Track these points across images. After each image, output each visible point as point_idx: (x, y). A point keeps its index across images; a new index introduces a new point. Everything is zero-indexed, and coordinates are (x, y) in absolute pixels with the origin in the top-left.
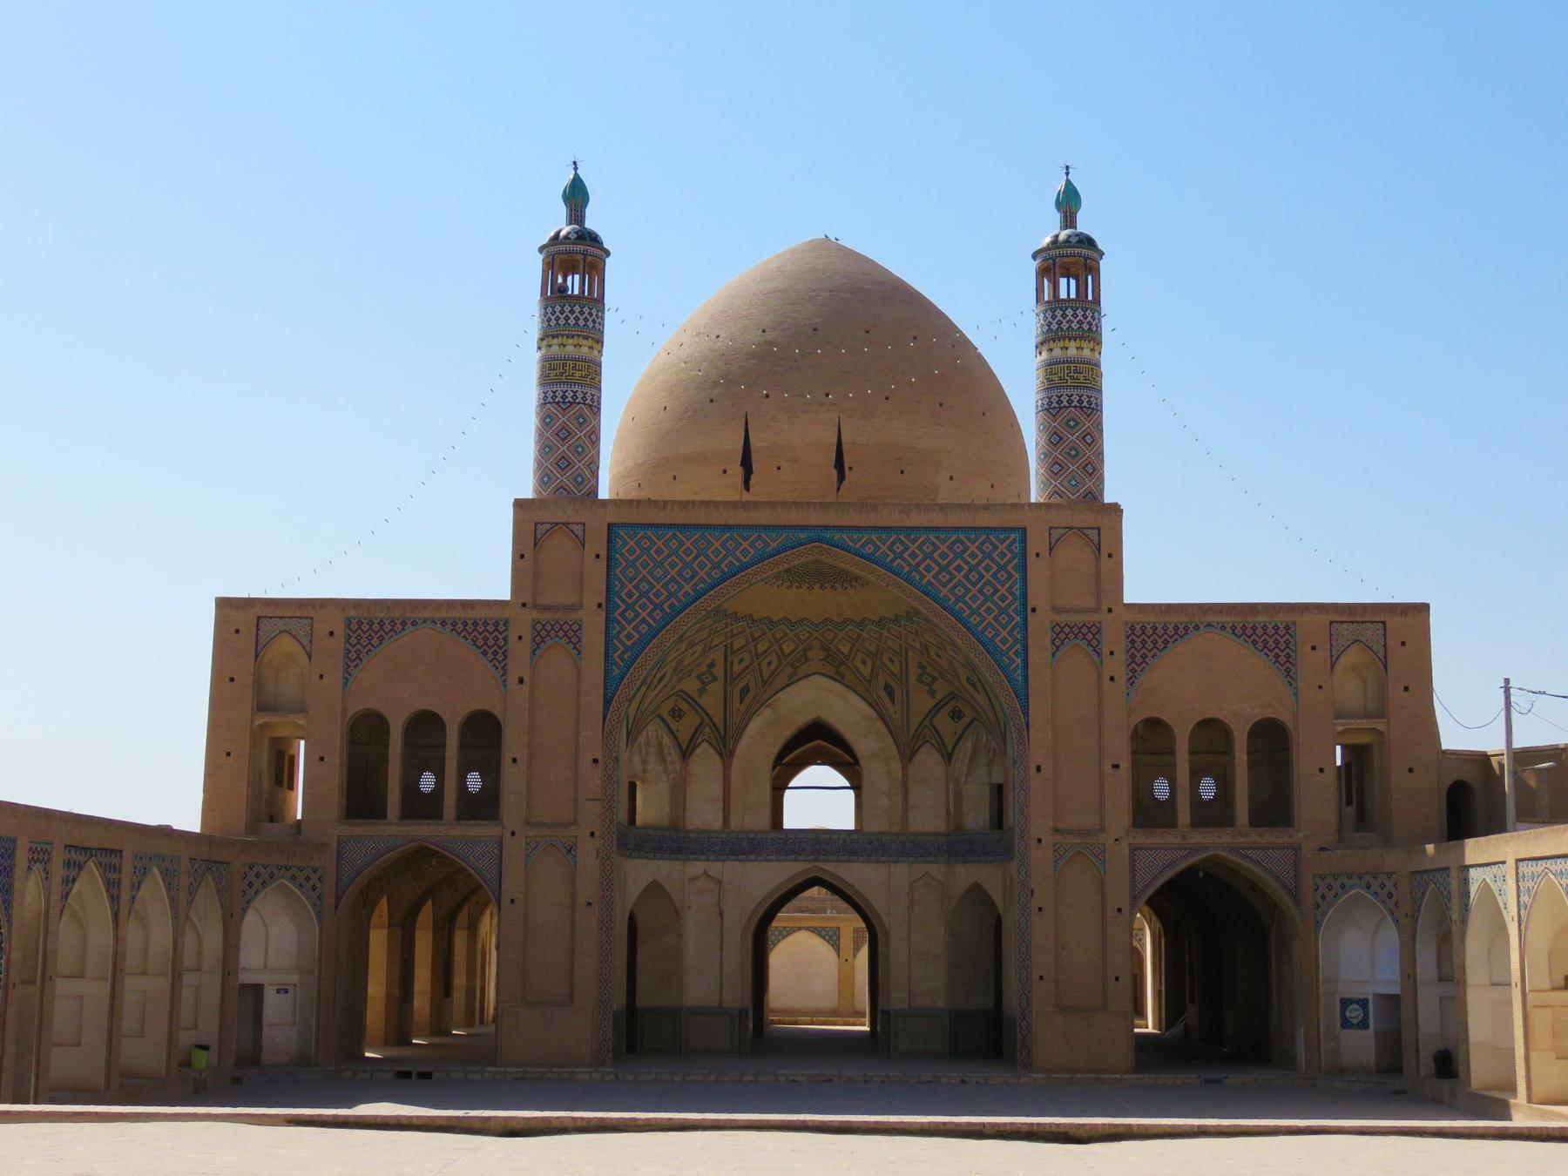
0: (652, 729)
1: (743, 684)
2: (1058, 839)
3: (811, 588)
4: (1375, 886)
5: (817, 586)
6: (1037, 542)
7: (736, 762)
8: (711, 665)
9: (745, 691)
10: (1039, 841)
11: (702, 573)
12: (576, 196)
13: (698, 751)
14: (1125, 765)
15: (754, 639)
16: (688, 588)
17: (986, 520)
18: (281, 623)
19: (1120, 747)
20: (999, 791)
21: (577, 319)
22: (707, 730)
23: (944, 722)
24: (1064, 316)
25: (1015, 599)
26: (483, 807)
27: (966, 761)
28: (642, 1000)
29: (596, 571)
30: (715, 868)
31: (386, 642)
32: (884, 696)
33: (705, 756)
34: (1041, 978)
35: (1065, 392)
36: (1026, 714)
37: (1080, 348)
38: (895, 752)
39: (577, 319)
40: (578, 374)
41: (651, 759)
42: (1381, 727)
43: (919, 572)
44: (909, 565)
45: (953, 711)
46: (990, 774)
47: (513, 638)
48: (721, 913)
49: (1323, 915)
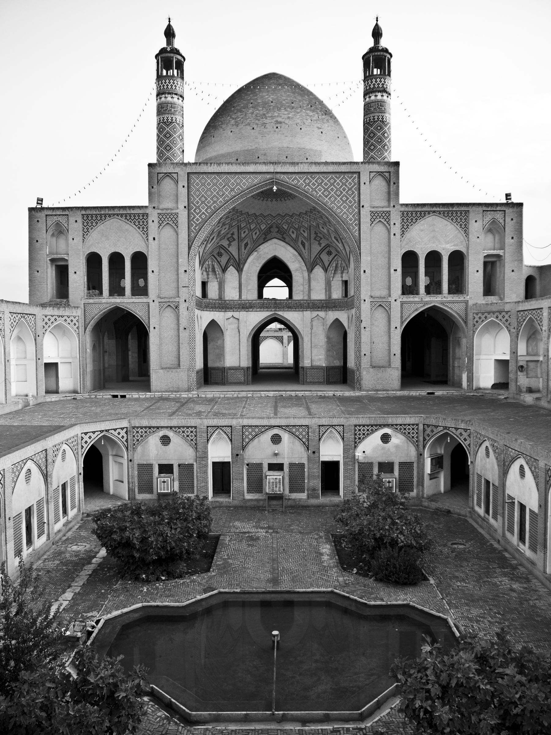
1: (245, 242)
2: (372, 300)
3: (272, 201)
4: (500, 317)
5: (274, 200)
6: (364, 178)
8: (233, 234)
9: (246, 245)
10: (365, 300)
11: (227, 193)
12: (169, 33)
13: (229, 269)
15: (249, 223)
16: (221, 199)
18: (55, 217)
19: (397, 263)
20: (346, 283)
21: (172, 86)
23: (325, 257)
24: (376, 81)
25: (355, 202)
26: (140, 291)
27: (333, 272)
28: (210, 365)
29: (183, 192)
30: (236, 314)
31: (99, 224)
32: (301, 246)
33: (232, 270)
34: (365, 355)
35: (376, 114)
36: (360, 249)
37: (382, 96)
38: (305, 268)
39: (172, 86)
40: (173, 110)
41: (210, 273)
42: (501, 254)
43: (316, 192)
44: (312, 188)
45: (328, 252)
46: (342, 277)
47: (150, 222)
48: (239, 331)
49: (476, 329)
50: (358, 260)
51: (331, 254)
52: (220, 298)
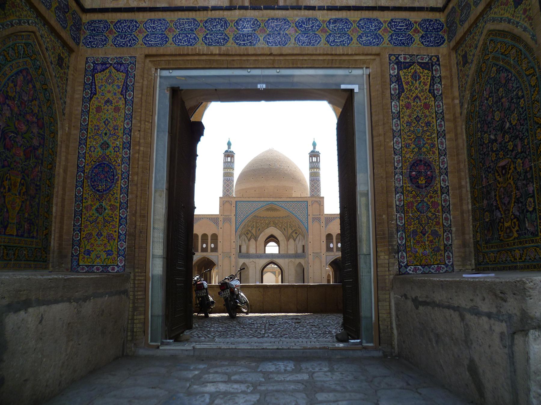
0: (244, 237)
6: (310, 203)
9: (259, 229)
14: (325, 241)
17: (301, 200)
19: (324, 238)
23: (294, 235)
26: (215, 250)
30: (254, 260)
33: (253, 241)
50: (308, 238)
52: (247, 253)
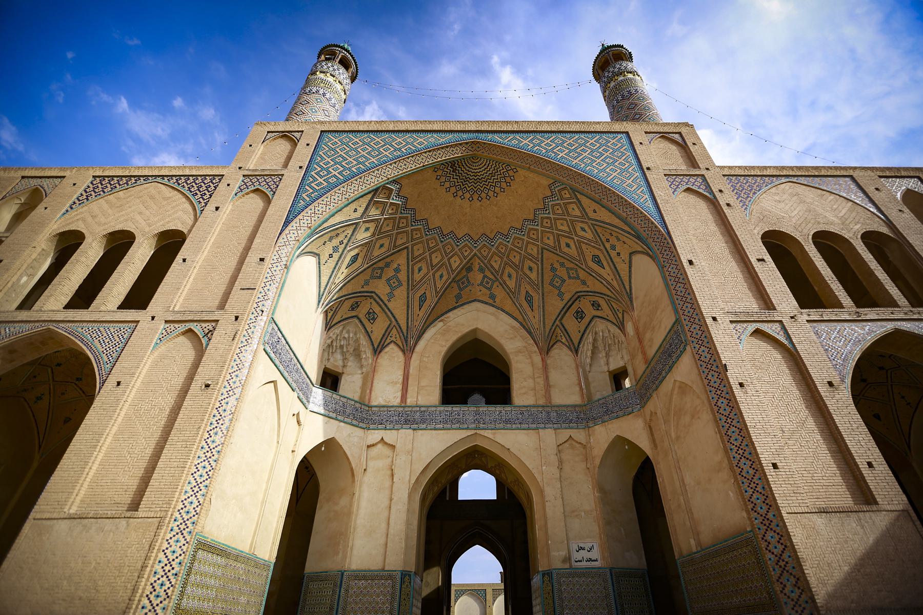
3: (471, 199)
5: (476, 196)
7: (415, 356)
8: (397, 270)
9: (423, 299)
22: (394, 331)
23: (570, 323)
32: (525, 304)
45: (577, 312)
51: (582, 318)
